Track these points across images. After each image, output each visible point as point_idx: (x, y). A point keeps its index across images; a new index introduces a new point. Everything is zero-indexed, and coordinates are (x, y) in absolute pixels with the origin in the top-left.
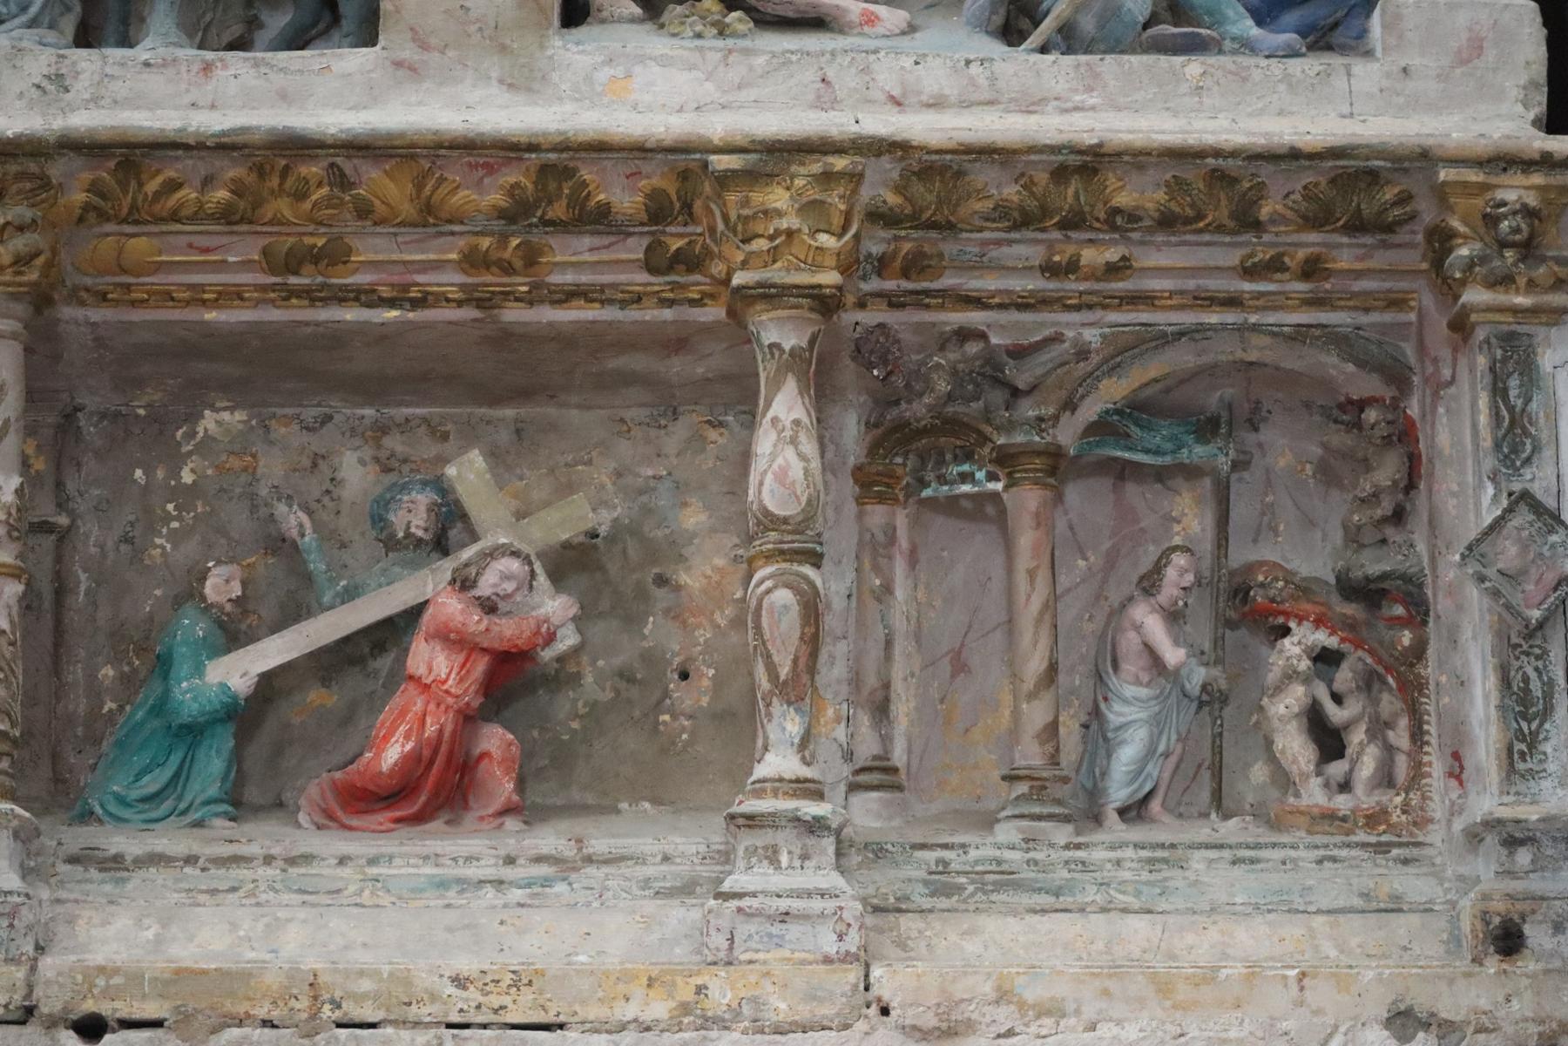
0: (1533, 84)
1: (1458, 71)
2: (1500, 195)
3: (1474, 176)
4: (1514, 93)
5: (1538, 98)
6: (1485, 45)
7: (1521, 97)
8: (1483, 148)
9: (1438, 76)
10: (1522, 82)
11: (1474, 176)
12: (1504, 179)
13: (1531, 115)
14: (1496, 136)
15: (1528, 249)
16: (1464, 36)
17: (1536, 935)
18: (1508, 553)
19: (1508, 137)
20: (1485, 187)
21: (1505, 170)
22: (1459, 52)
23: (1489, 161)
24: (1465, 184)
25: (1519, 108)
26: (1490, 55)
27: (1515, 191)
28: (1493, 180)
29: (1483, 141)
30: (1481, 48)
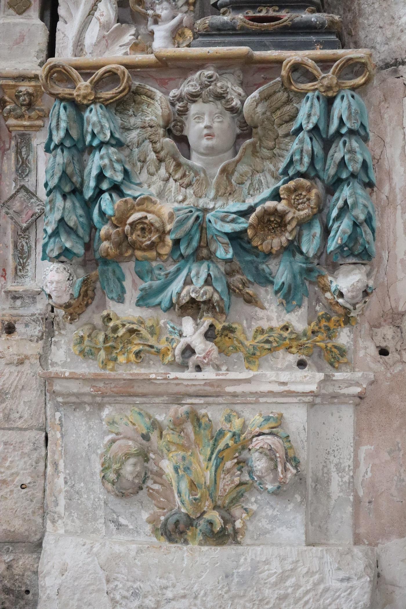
0: (41, 51)
1: (15, 47)
2: (21, 89)
3: (11, 83)
4: (34, 54)
5: (43, 55)
6: (25, 37)
7: (36, 55)
8: (15, 73)
9: (9, 48)
10: (37, 50)
11: (11, 83)
12: (22, 83)
13: (39, 61)
14: (21, 69)
15: (30, 106)
16: (18, 35)
17: (19, 328)
18: (16, 205)
19: (25, 69)
20: (15, 86)
21: (23, 80)
22: (16, 40)
23: (17, 78)
24: (9, 85)
25: (35, 59)
26: (26, 41)
27: (25, 87)
28: (18, 84)
29: (15, 71)
30: (24, 38)
